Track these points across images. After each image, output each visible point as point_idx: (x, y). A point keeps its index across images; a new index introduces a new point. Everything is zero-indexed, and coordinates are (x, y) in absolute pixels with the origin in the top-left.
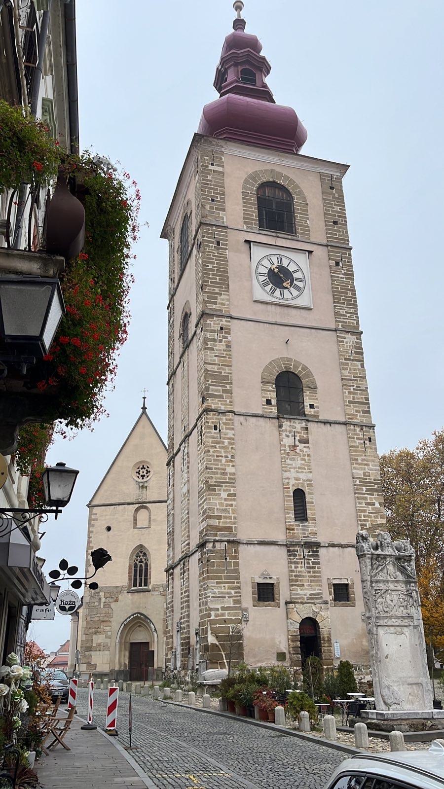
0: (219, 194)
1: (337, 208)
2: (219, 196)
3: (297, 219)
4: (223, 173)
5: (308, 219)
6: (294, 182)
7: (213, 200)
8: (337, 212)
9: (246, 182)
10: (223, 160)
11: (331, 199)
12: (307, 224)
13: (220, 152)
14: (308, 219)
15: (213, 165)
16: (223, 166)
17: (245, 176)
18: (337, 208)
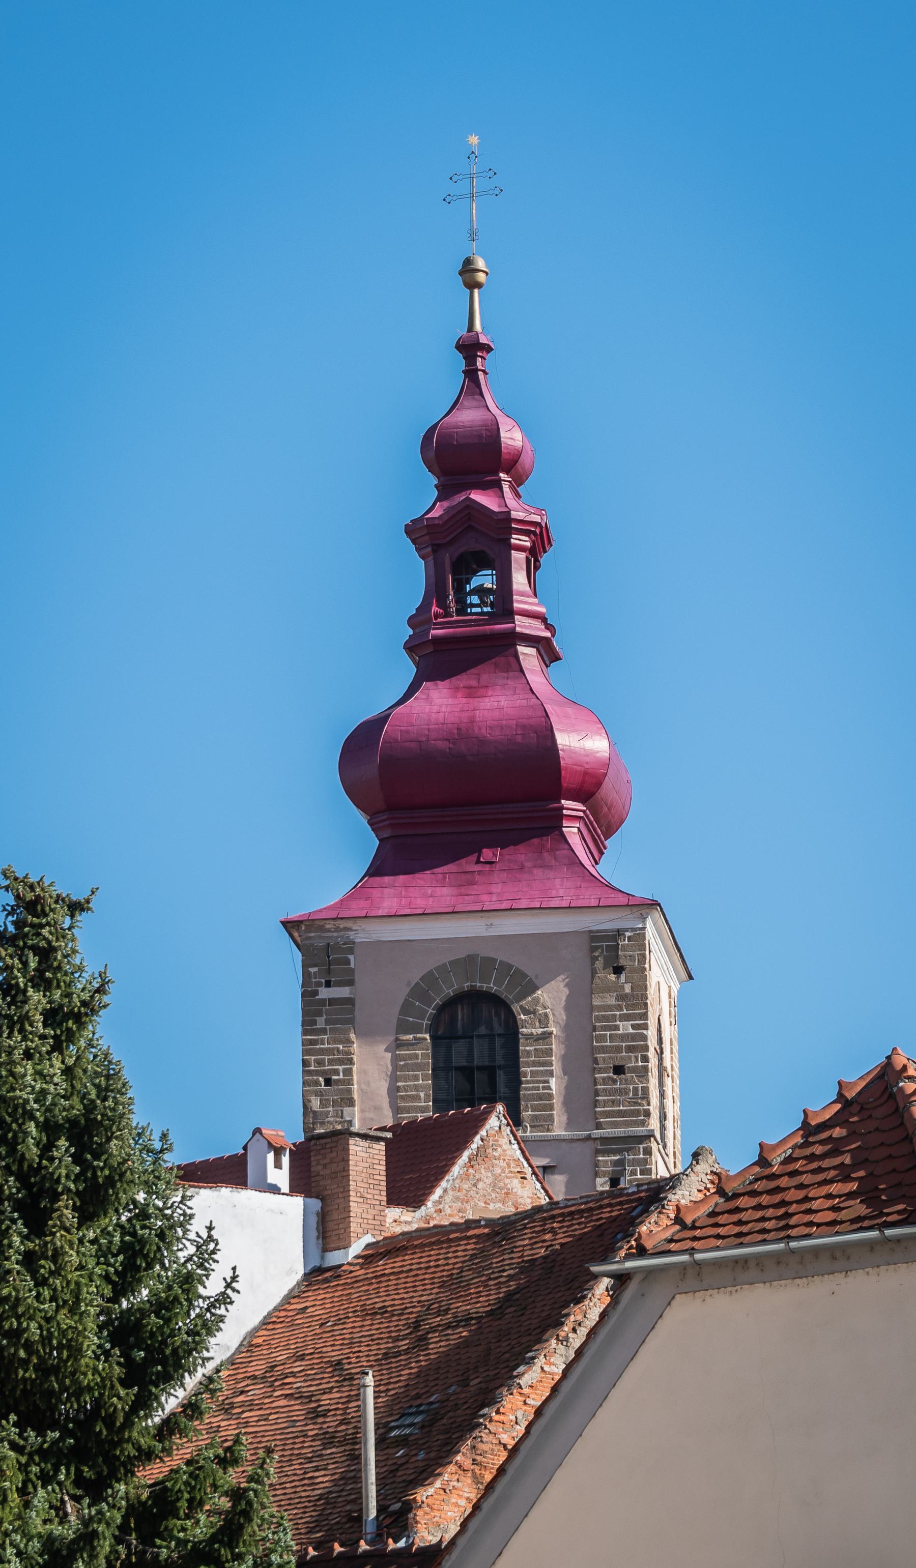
0: (341, 1062)
1: (626, 1027)
2: (341, 1068)
3: (528, 1082)
4: (350, 1001)
5: (551, 1074)
6: (525, 976)
7: (328, 1082)
8: (624, 1037)
9: (406, 1008)
10: (352, 966)
11: (612, 1001)
12: (549, 1088)
13: (345, 944)
14: (551, 1074)
15: (328, 984)
16: (350, 983)
17: (402, 994)
18: (626, 1027)
